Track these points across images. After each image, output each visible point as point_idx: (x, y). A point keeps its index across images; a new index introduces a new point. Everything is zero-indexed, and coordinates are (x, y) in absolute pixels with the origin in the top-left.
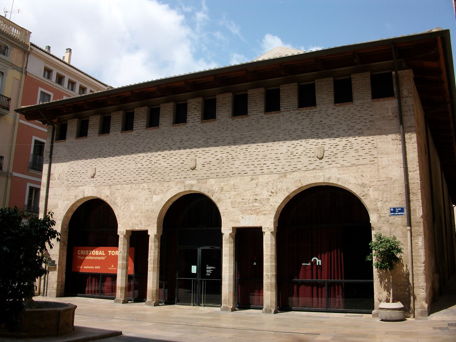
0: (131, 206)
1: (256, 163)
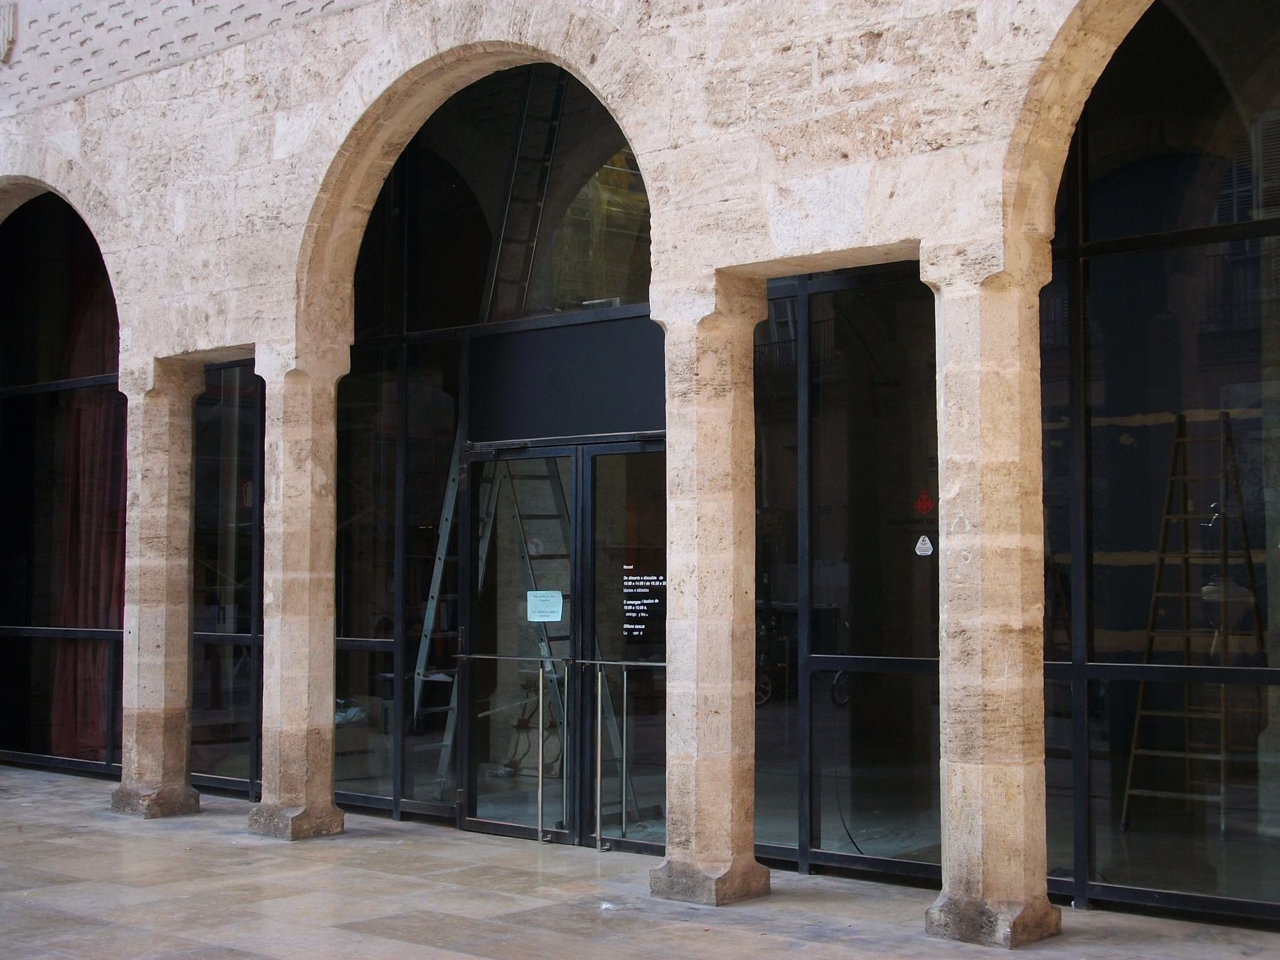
0: (172, 205)
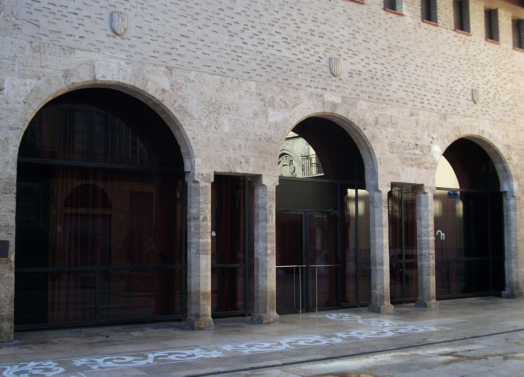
1: (416, 91)
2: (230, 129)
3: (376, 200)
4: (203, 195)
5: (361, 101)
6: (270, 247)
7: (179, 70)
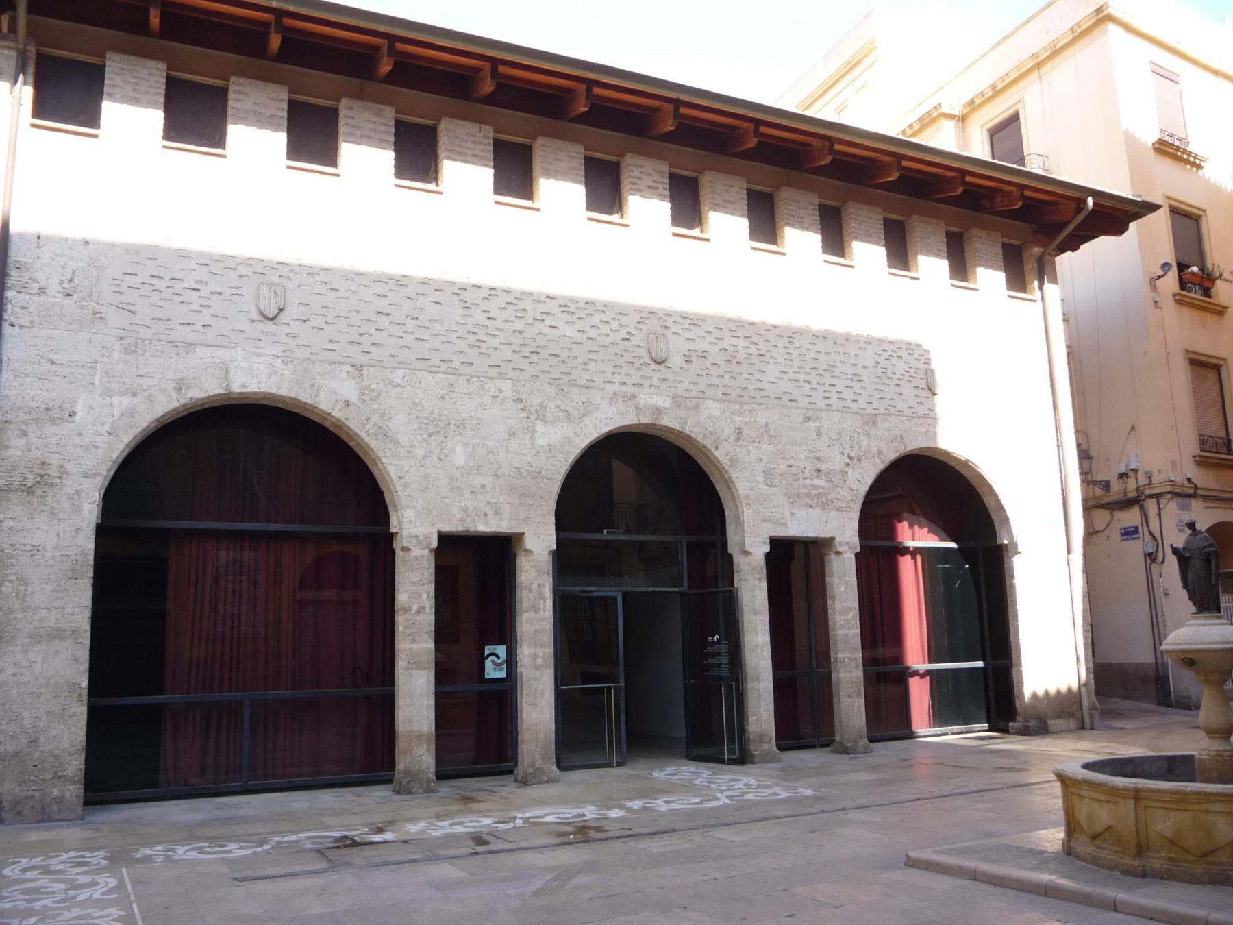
0: (453, 450)
1: (814, 380)
2: (466, 459)
3: (742, 567)
4: (418, 571)
5: (709, 402)
6: (541, 654)
7: (372, 369)
